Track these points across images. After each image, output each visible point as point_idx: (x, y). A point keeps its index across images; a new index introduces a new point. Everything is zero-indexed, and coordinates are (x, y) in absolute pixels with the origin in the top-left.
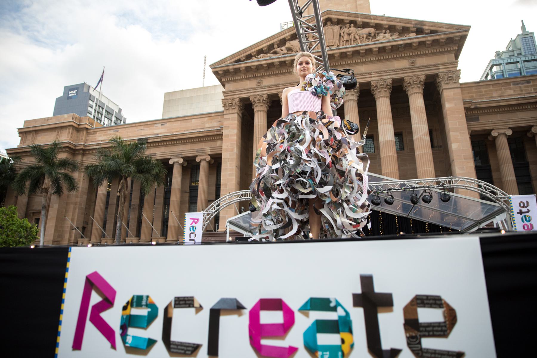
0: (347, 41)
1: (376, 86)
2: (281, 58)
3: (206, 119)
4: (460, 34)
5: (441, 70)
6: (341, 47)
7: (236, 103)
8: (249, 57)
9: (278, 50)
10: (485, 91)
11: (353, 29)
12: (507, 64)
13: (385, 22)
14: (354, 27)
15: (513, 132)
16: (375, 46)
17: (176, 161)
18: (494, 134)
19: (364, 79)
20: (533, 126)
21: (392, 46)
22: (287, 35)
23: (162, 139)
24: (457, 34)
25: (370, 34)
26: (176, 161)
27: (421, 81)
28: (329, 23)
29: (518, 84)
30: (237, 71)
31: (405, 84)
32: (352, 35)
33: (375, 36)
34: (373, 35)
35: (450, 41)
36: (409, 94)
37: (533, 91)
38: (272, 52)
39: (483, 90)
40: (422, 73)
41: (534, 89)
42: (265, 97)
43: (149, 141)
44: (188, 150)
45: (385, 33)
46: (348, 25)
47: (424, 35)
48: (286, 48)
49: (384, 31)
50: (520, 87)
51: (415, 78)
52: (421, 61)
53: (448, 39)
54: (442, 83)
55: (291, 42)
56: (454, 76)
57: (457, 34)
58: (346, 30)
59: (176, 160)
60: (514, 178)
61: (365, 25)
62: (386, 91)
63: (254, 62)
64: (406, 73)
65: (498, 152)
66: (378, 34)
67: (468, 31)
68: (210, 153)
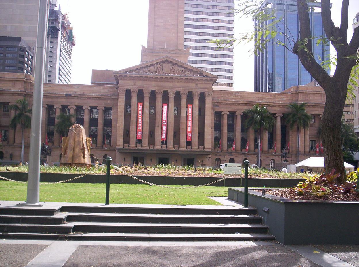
3: (102, 87)
4: (215, 79)
5: (207, 91)
9: (144, 70)
10: (223, 95)
11: (176, 67)
12: (277, 4)
13: (189, 68)
15: (230, 113)
17: (86, 107)
20: (237, 112)
22: (149, 64)
26: (86, 107)
32: (176, 70)
33: (184, 72)
38: (142, 70)
39: (223, 94)
41: (240, 97)
42: (138, 91)
44: (93, 103)
45: (188, 71)
47: (202, 77)
50: (236, 95)
59: (86, 107)
60: (227, 131)
63: (134, 74)
65: (224, 120)
68: (104, 106)
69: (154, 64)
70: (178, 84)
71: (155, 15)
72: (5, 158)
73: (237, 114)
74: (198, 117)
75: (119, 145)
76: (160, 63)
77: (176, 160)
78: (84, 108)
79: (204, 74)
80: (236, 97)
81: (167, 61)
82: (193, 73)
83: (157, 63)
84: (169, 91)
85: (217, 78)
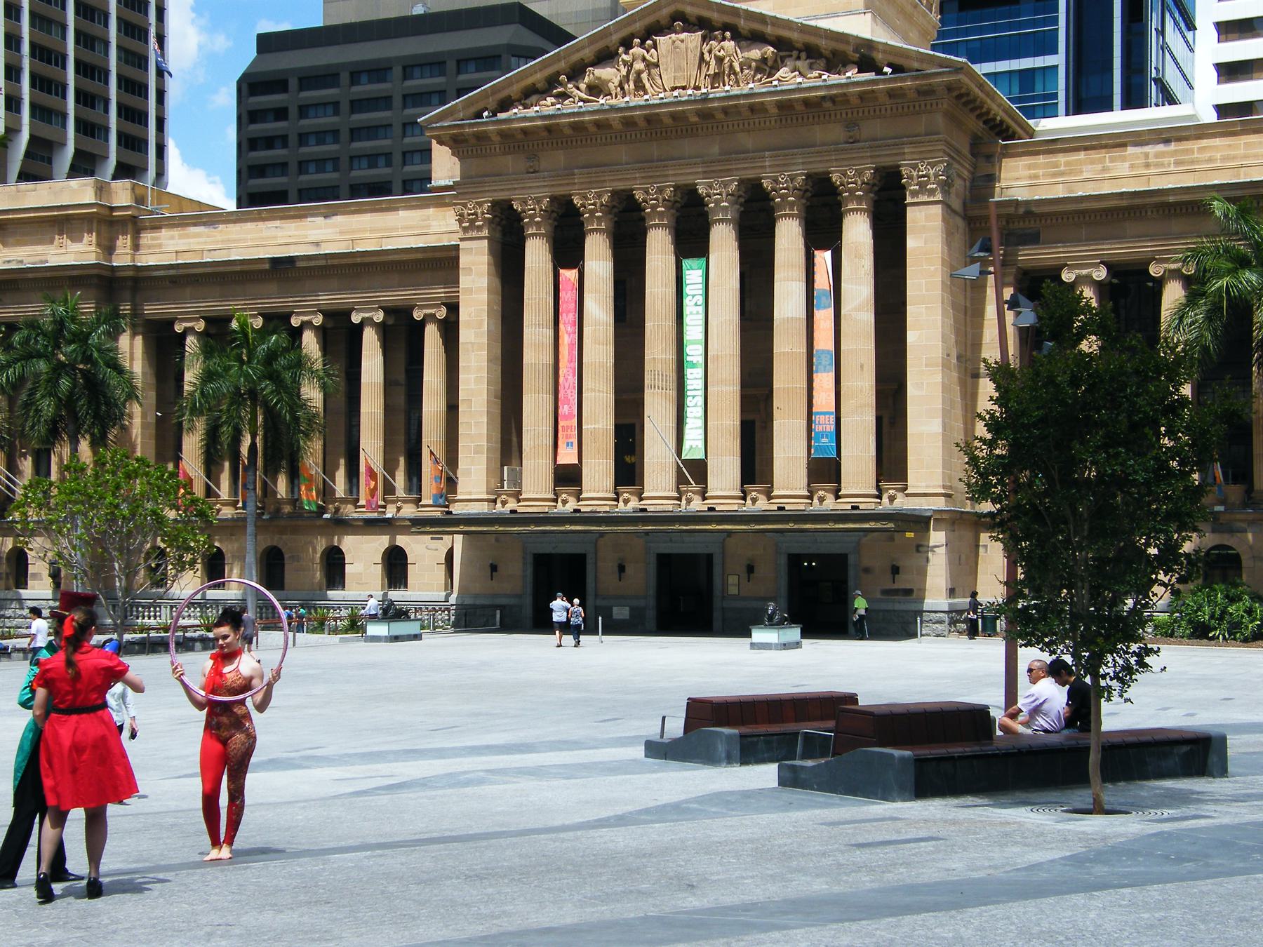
2: (573, 114)
7: (483, 213)
8: (505, 105)
10: (1067, 164)
11: (729, 45)
13: (795, 36)
14: (732, 38)
23: (330, 262)
25: (764, 60)
30: (481, 138)
33: (775, 68)
34: (770, 63)
35: (926, 93)
37: (1172, 168)
41: (1177, 163)
43: (300, 264)
45: (798, 58)
49: (795, 53)
50: (1147, 155)
61: (756, 38)
72: (35, 576)
75: (470, 493)
77: (751, 569)
78: (356, 318)
79: (879, 57)
81: (679, 16)
82: (822, 63)
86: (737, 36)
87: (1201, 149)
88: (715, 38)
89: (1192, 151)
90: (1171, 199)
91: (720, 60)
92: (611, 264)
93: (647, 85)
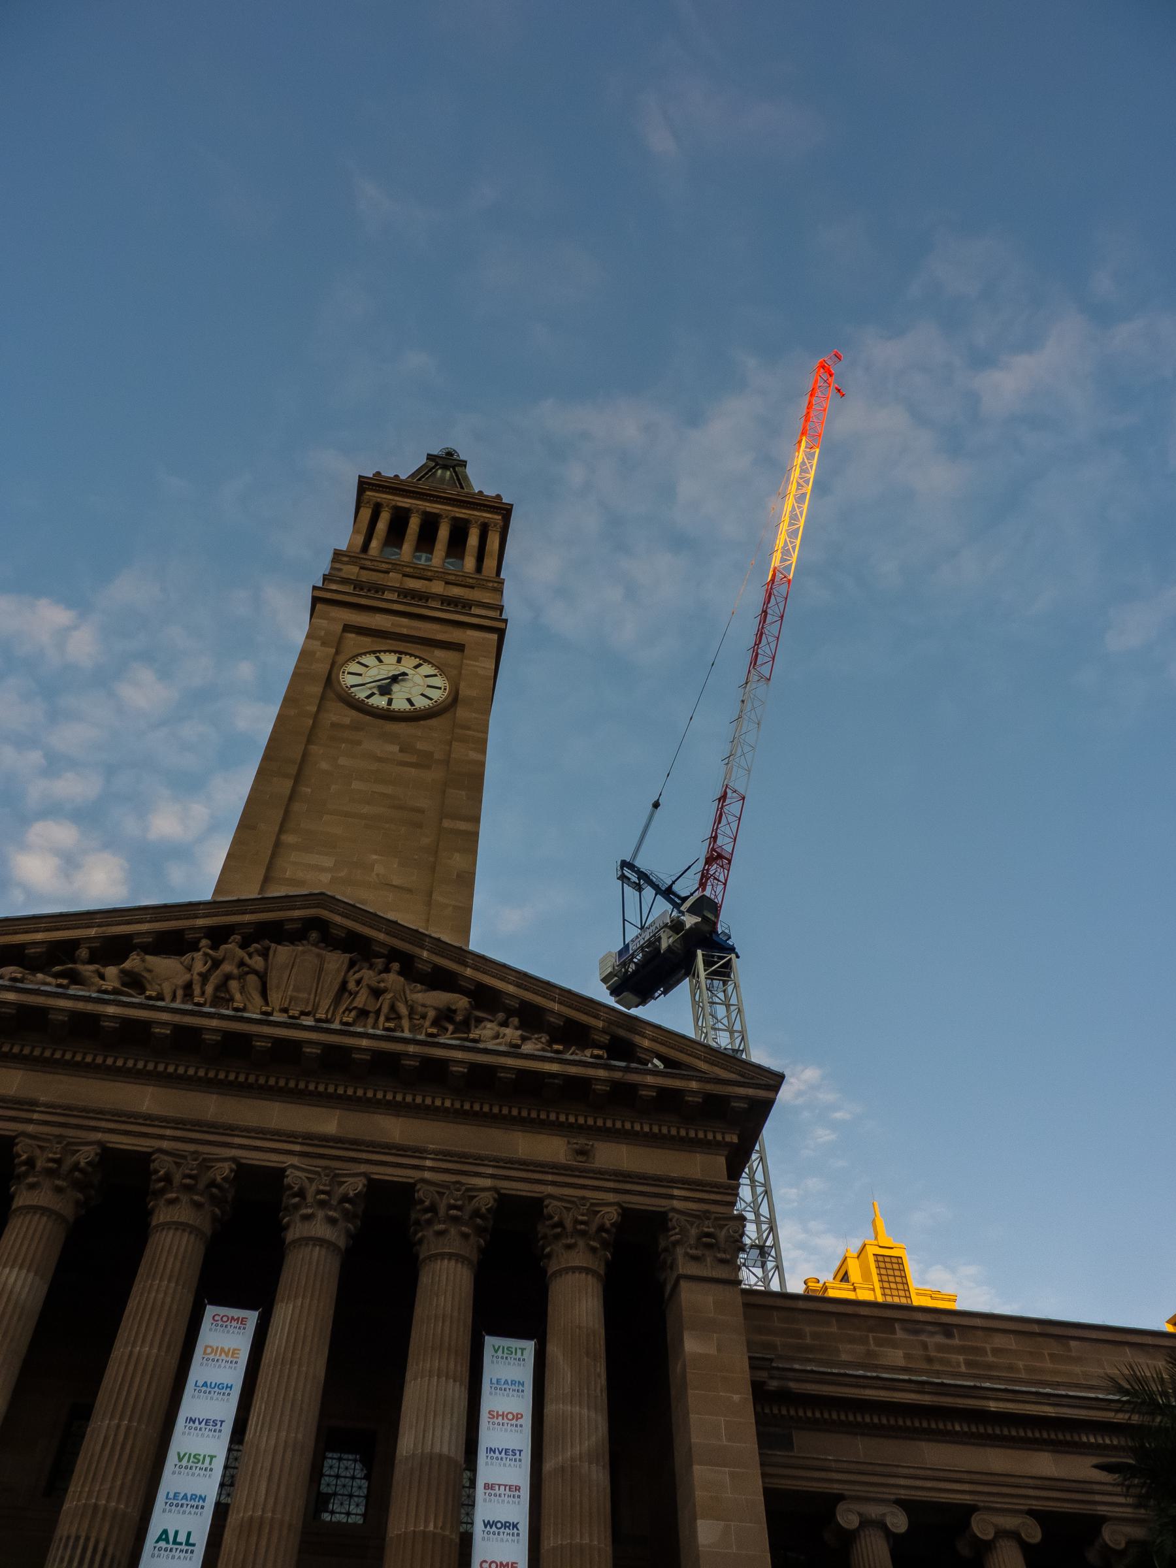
0: (363, 1013)
1: (433, 1209)
4: (750, 1092)
5: (679, 1202)
6: (336, 1026)
9: (87, 970)
11: (393, 979)
13: (511, 989)
14: (400, 973)
16: (459, 1055)
18: (847, 1518)
19: (390, 1170)
21: (522, 1073)
22: (144, 927)
24: (742, 1091)
27: (602, 1228)
28: (314, 935)
29: (916, 1332)
31: (542, 1229)
32: (389, 996)
33: (465, 1026)
34: (459, 1018)
35: (715, 1109)
36: (553, 1267)
39: (807, 1329)
40: (611, 1197)
41: (969, 1364)
45: (504, 1024)
46: (380, 962)
48: (123, 971)
49: (501, 1016)
50: (925, 1346)
51: (584, 1209)
52: (613, 1155)
53: (709, 1098)
54: (680, 1251)
55: (148, 957)
56: (722, 1234)
57: (742, 1091)
58: (368, 975)
61: (440, 980)
62: (465, 1236)
64: (553, 1183)
66: (479, 1021)
67: (776, 1089)
69: (189, 936)
70: (394, 1128)
71: (281, 830)
73: (982, 1527)
74: (599, 1476)
76: (244, 946)
79: (646, 1043)
80: (929, 1360)
83: (218, 936)
84: (293, 1178)
85: (767, 1089)
86: (408, 967)
87: (996, 1351)
88: (371, 967)
89: (980, 1351)
90: (993, 1406)
91: (377, 993)
92: (45, 1289)
93: (238, 996)
